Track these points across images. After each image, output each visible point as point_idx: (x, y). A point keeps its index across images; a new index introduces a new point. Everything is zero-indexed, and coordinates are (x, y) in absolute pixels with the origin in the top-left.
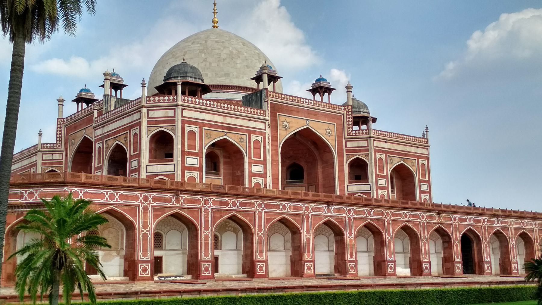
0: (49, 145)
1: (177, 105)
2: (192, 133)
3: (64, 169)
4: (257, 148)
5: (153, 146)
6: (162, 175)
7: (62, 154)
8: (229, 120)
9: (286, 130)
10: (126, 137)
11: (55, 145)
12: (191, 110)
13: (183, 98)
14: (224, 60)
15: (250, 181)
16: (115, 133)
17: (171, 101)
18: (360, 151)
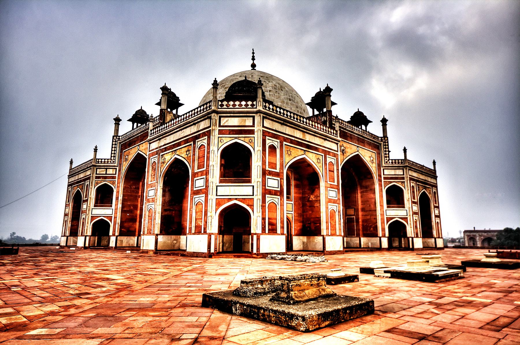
6: (236, 199)
7: (116, 169)
8: (308, 137)
10: (189, 151)
11: (109, 161)
13: (264, 104)
17: (250, 106)
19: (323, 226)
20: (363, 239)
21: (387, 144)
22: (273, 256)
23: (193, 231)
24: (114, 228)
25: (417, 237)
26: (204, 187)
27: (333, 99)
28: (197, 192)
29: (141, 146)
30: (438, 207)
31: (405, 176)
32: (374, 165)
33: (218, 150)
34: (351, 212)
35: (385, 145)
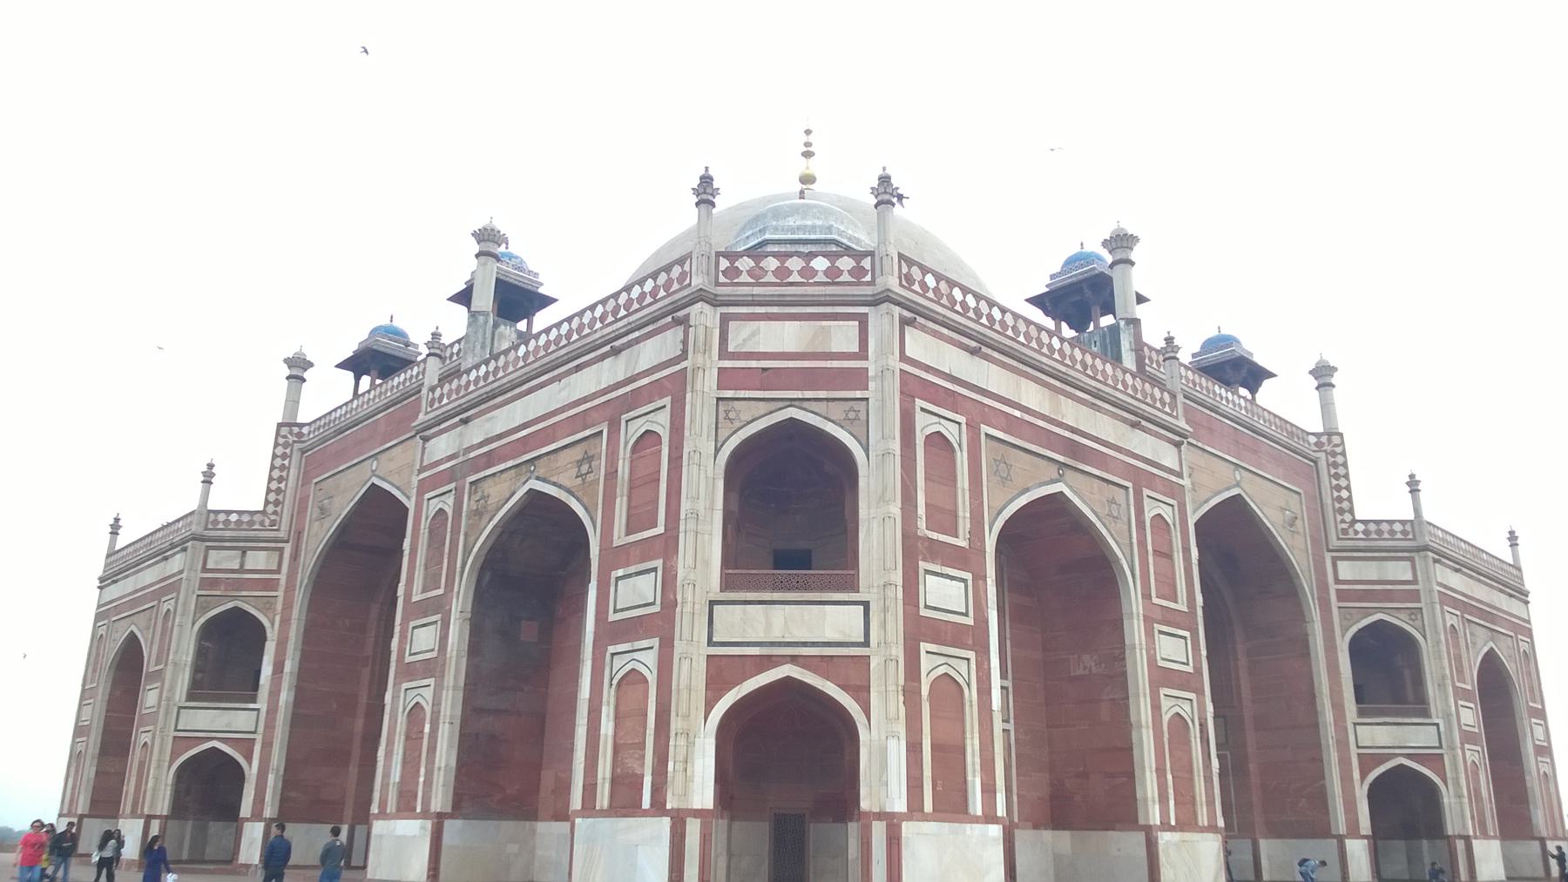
0: (234, 517)
1: (884, 298)
2: (938, 441)
3: (279, 607)
4: (1165, 555)
6: (794, 659)
7: (281, 550)
8: (1073, 414)
10: (588, 458)
11: (257, 518)
12: (935, 334)
13: (905, 270)
15: (1156, 707)
16: (525, 444)
17: (845, 277)
18: (1388, 596)
19: (1149, 785)
20: (1264, 844)
21: (1340, 459)
24: (261, 790)
25: (1485, 835)
26: (656, 609)
27: (1139, 278)
29: (384, 457)
30: (1541, 714)
32: (1299, 542)
33: (717, 450)
35: (1335, 465)
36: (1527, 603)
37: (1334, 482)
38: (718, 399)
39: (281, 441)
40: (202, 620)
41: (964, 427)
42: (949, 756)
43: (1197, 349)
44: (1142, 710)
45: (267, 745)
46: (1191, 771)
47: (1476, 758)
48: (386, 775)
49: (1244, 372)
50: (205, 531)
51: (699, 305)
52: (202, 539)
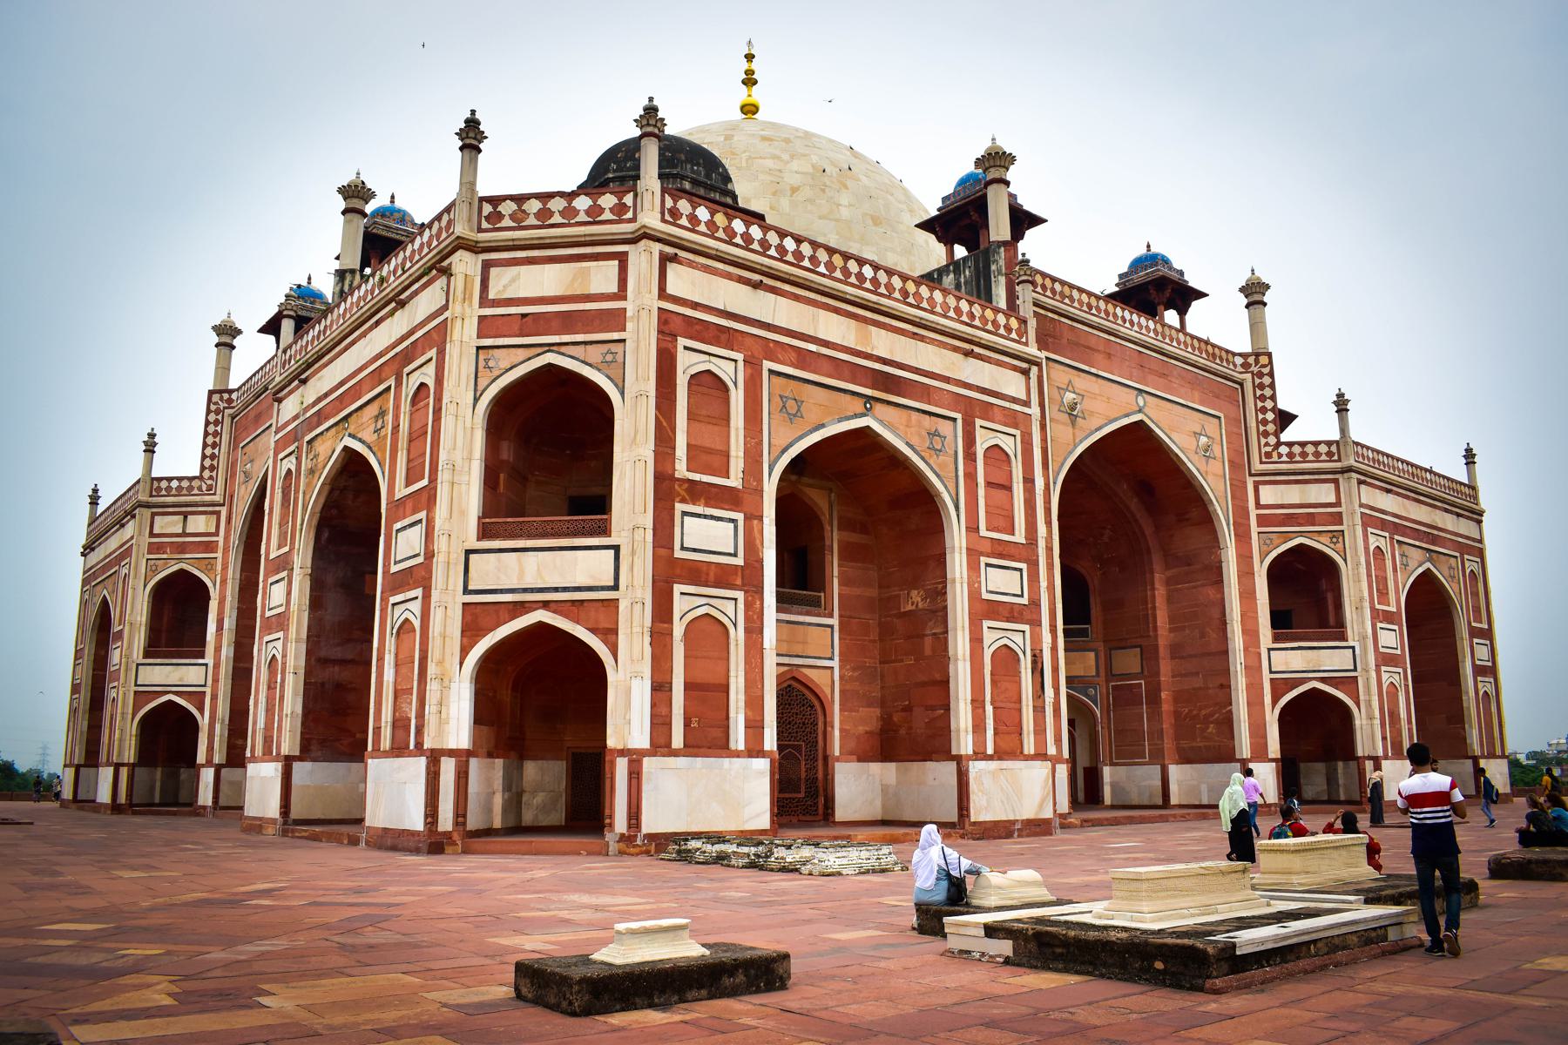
0: (175, 484)
3: (219, 568)
5: (507, 452)
6: (546, 605)
7: (218, 514)
8: (883, 343)
9: (1073, 424)
10: (382, 414)
11: (196, 483)
12: (707, 269)
13: (669, 203)
14: (794, 190)
15: (976, 640)
16: (342, 401)
17: (607, 215)
18: (1311, 519)
19: (962, 716)
20: (1175, 771)
21: (1267, 380)
22: (693, 844)
23: (386, 744)
26: (420, 560)
28: (402, 581)
30: (1488, 634)
31: (1342, 509)
33: (476, 400)
34: (1129, 661)
36: (1479, 522)
37: (1260, 404)
38: (478, 348)
39: (213, 407)
40: (153, 582)
41: (741, 364)
42: (708, 696)
43: (1125, 270)
44: (960, 644)
45: (214, 697)
46: (1020, 701)
47: (1396, 679)
48: (255, 723)
49: (1168, 293)
50: (152, 496)
51: (460, 253)
52: (147, 506)
